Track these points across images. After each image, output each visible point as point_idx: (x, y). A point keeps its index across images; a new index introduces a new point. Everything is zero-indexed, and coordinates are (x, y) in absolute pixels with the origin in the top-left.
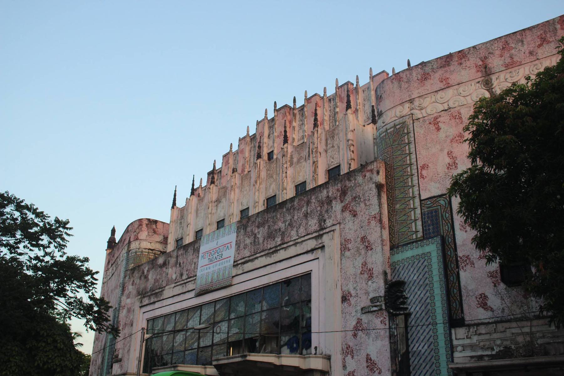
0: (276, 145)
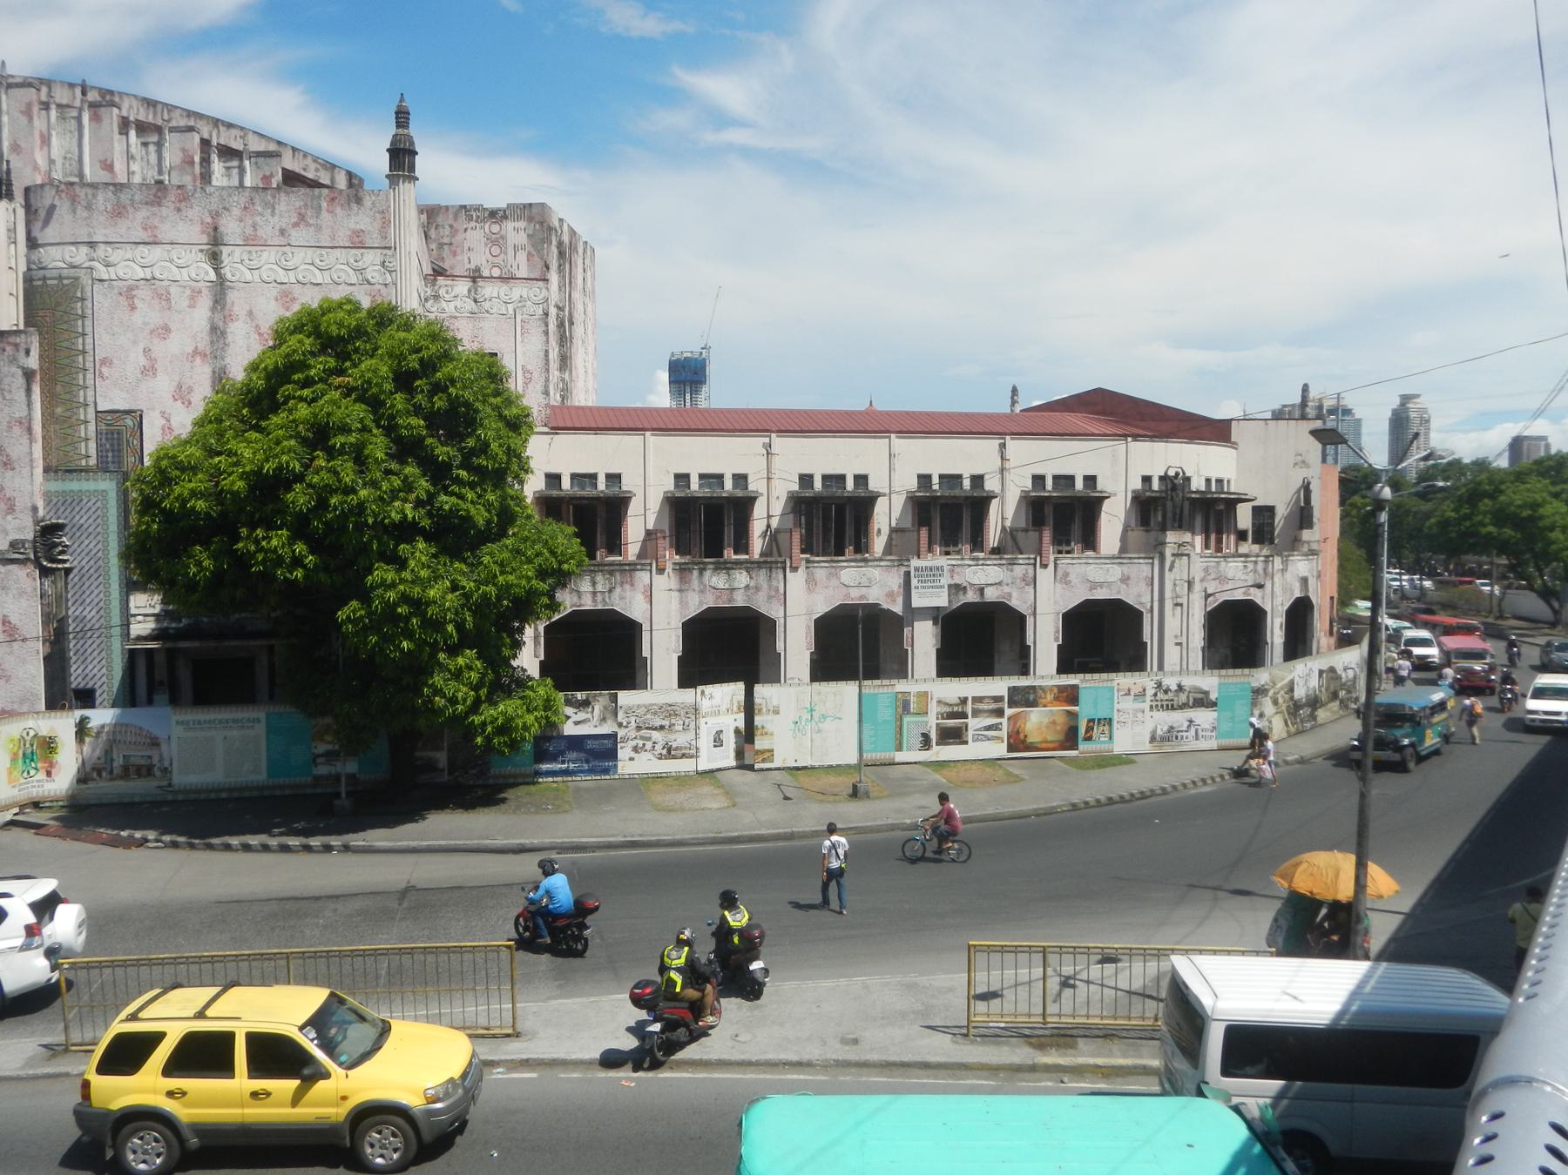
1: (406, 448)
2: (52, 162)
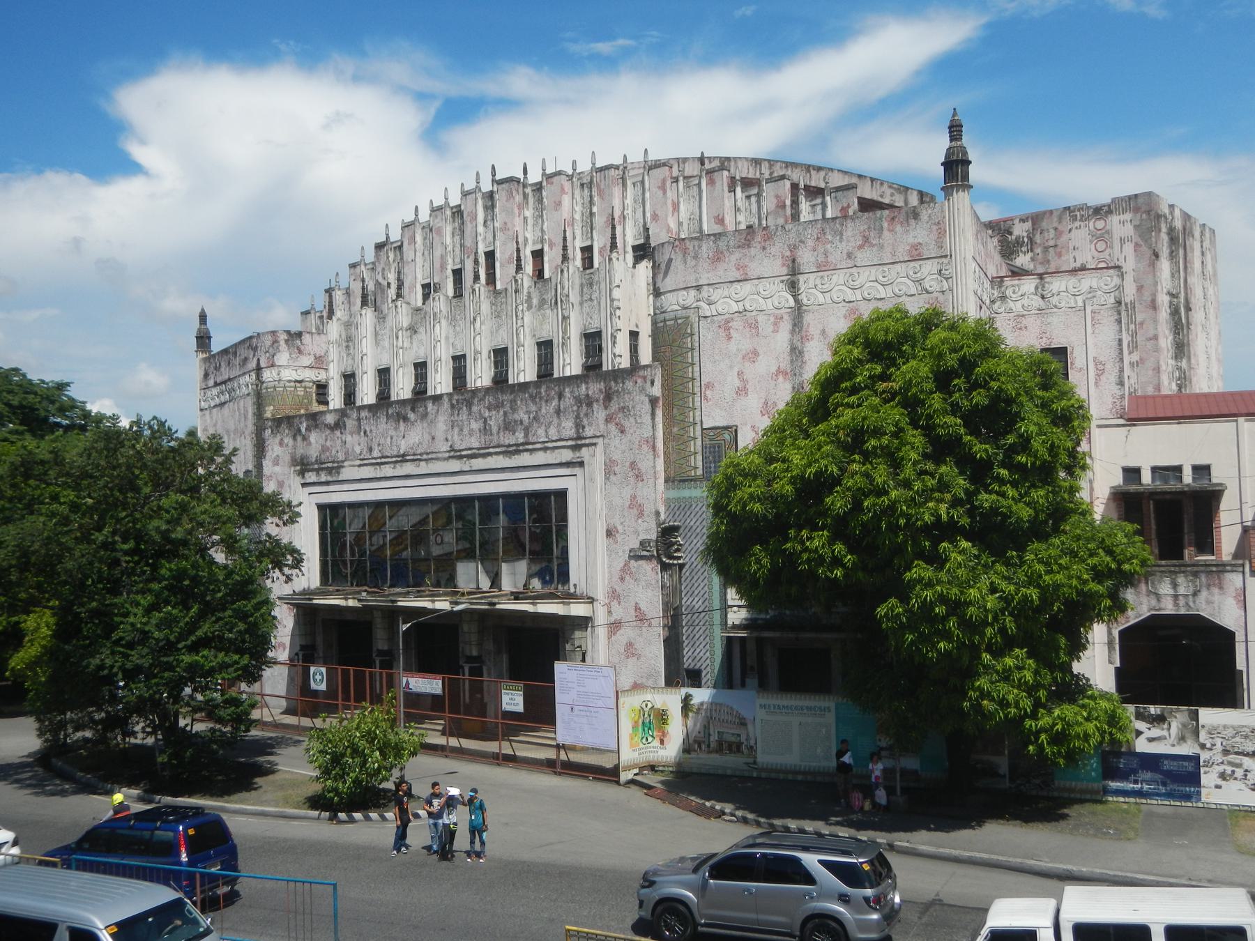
0: (498, 243)
1: (942, 448)
2: (680, 224)
